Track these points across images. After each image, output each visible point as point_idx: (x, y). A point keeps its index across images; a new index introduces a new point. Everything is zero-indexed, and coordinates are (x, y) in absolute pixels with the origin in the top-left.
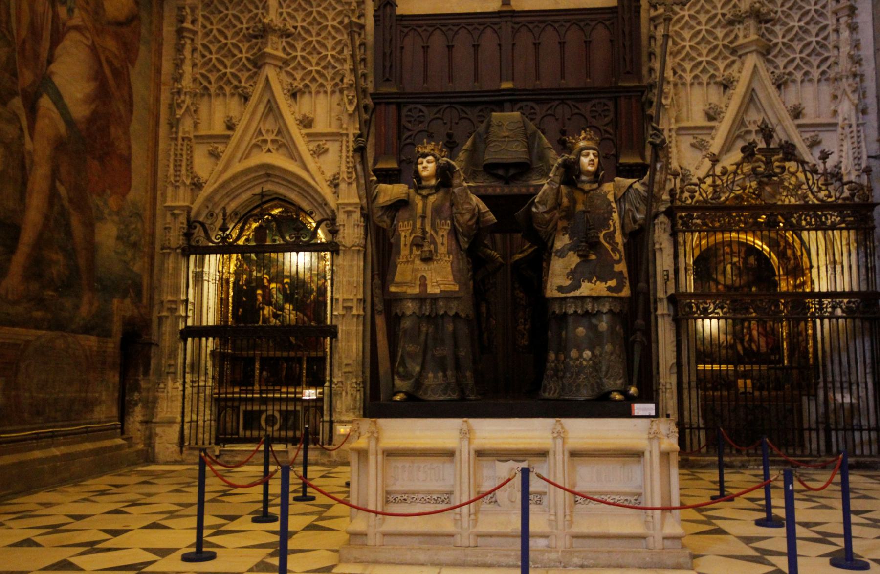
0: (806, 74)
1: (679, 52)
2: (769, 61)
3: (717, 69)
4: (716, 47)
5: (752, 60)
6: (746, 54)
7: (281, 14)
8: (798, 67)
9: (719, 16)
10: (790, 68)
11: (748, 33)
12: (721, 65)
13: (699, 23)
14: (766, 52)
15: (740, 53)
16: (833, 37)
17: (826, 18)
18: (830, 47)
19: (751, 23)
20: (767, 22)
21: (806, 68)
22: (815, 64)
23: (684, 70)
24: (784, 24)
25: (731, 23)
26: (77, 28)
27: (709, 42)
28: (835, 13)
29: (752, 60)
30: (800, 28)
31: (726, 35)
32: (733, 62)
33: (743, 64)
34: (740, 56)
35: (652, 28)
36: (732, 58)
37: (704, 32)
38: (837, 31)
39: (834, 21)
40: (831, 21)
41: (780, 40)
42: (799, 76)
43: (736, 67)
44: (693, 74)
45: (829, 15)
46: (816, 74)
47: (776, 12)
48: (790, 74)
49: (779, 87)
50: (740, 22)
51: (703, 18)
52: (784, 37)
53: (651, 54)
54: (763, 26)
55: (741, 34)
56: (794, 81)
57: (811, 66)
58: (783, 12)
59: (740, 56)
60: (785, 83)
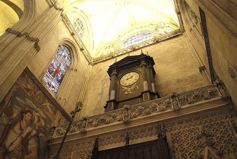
0: (228, 150)
1: (184, 150)
2: (214, 148)
3: (197, 153)
4: (195, 146)
5: (207, 148)
6: (205, 147)
7: (74, 156)
8: (225, 148)
9: (194, 137)
10: (222, 149)
11: (203, 140)
12: (198, 152)
13: (188, 141)
14: (212, 145)
15: (203, 147)
16: (233, 137)
17: (228, 132)
18: (233, 140)
19: (204, 137)
20: (210, 136)
21: (228, 148)
22: (231, 146)
23: (186, 156)
24: (216, 136)
25: (198, 138)
27: (192, 146)
28: (230, 129)
29: (207, 148)
30: (221, 136)
31: (198, 142)
32: (202, 150)
33: (205, 150)
34: (204, 148)
35: (173, 144)
36: (201, 149)
37: (190, 143)
38: (233, 134)
39: (231, 132)
40: (230, 132)
41: (216, 141)
42: (226, 151)
43: (203, 152)
44: (189, 156)
45: (229, 130)
46: (232, 149)
47: (212, 133)
48: (222, 151)
49: (220, 155)
50: (201, 138)
51: (189, 139)
52: (217, 140)
53: (174, 152)
54: (209, 137)
55: (202, 141)
56: (225, 153)
57: (230, 147)
58: (214, 133)
59: (204, 148)
60: (223, 154)
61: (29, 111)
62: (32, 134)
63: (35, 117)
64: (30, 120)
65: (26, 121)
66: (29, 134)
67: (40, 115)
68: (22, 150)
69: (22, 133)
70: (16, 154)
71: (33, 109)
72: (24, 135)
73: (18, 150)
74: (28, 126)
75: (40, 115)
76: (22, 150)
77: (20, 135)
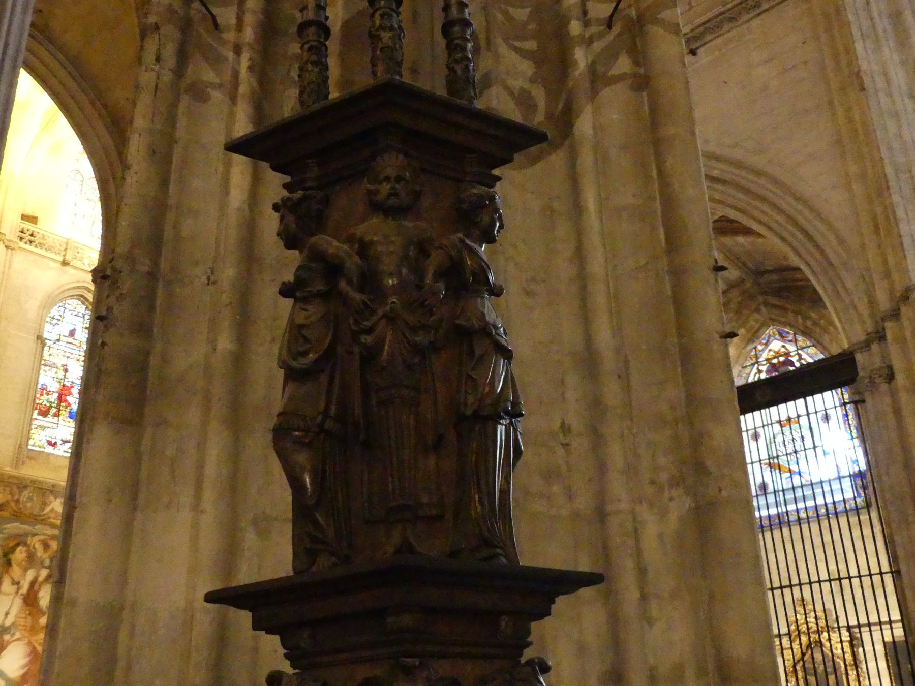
26: (18, 639)
61: (18, 545)
62: (41, 579)
63: (37, 546)
64: (26, 557)
65: (19, 565)
66: (33, 583)
67: (44, 537)
68: (30, 614)
69: (18, 589)
70: (20, 625)
71: (26, 534)
72: (25, 589)
73: (23, 618)
74: (26, 570)
75: (44, 537)
76: (30, 614)
77: (17, 593)
